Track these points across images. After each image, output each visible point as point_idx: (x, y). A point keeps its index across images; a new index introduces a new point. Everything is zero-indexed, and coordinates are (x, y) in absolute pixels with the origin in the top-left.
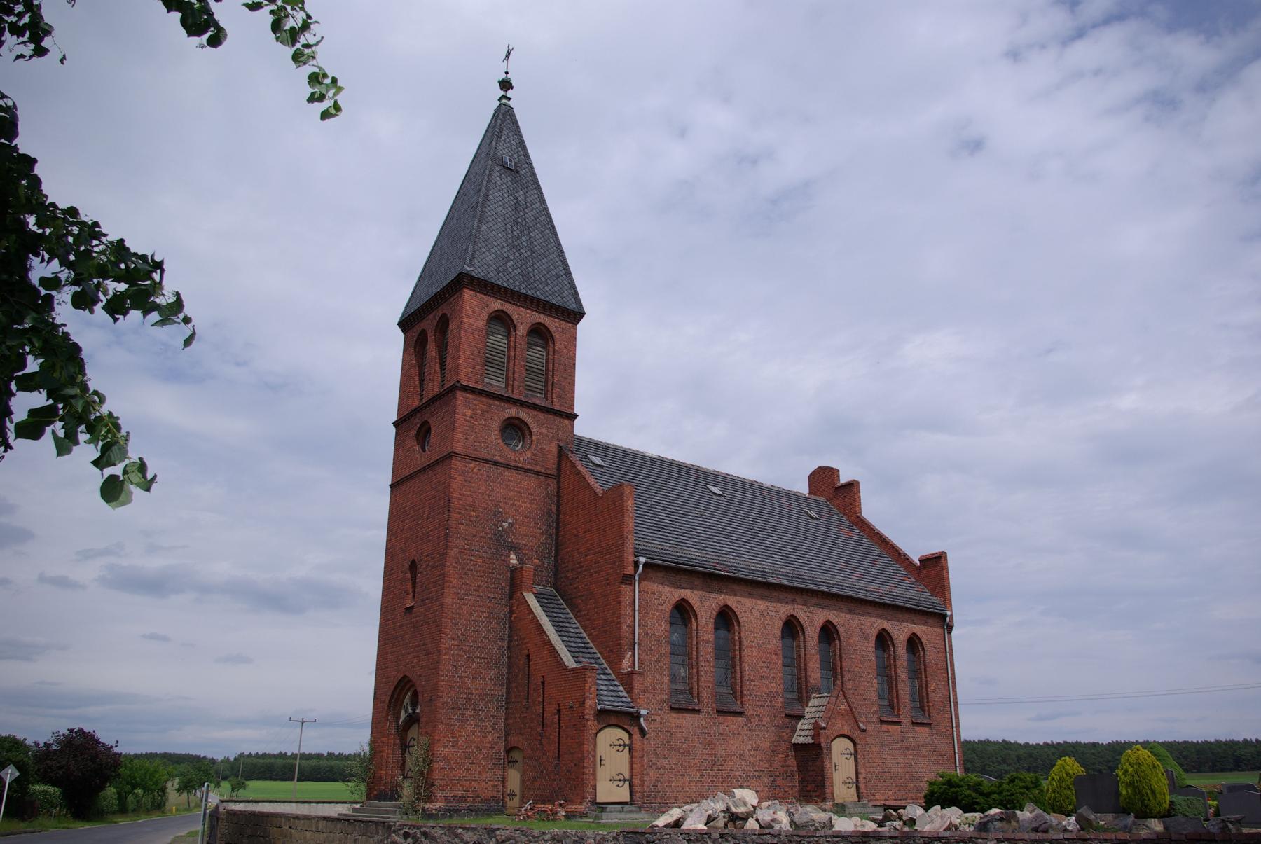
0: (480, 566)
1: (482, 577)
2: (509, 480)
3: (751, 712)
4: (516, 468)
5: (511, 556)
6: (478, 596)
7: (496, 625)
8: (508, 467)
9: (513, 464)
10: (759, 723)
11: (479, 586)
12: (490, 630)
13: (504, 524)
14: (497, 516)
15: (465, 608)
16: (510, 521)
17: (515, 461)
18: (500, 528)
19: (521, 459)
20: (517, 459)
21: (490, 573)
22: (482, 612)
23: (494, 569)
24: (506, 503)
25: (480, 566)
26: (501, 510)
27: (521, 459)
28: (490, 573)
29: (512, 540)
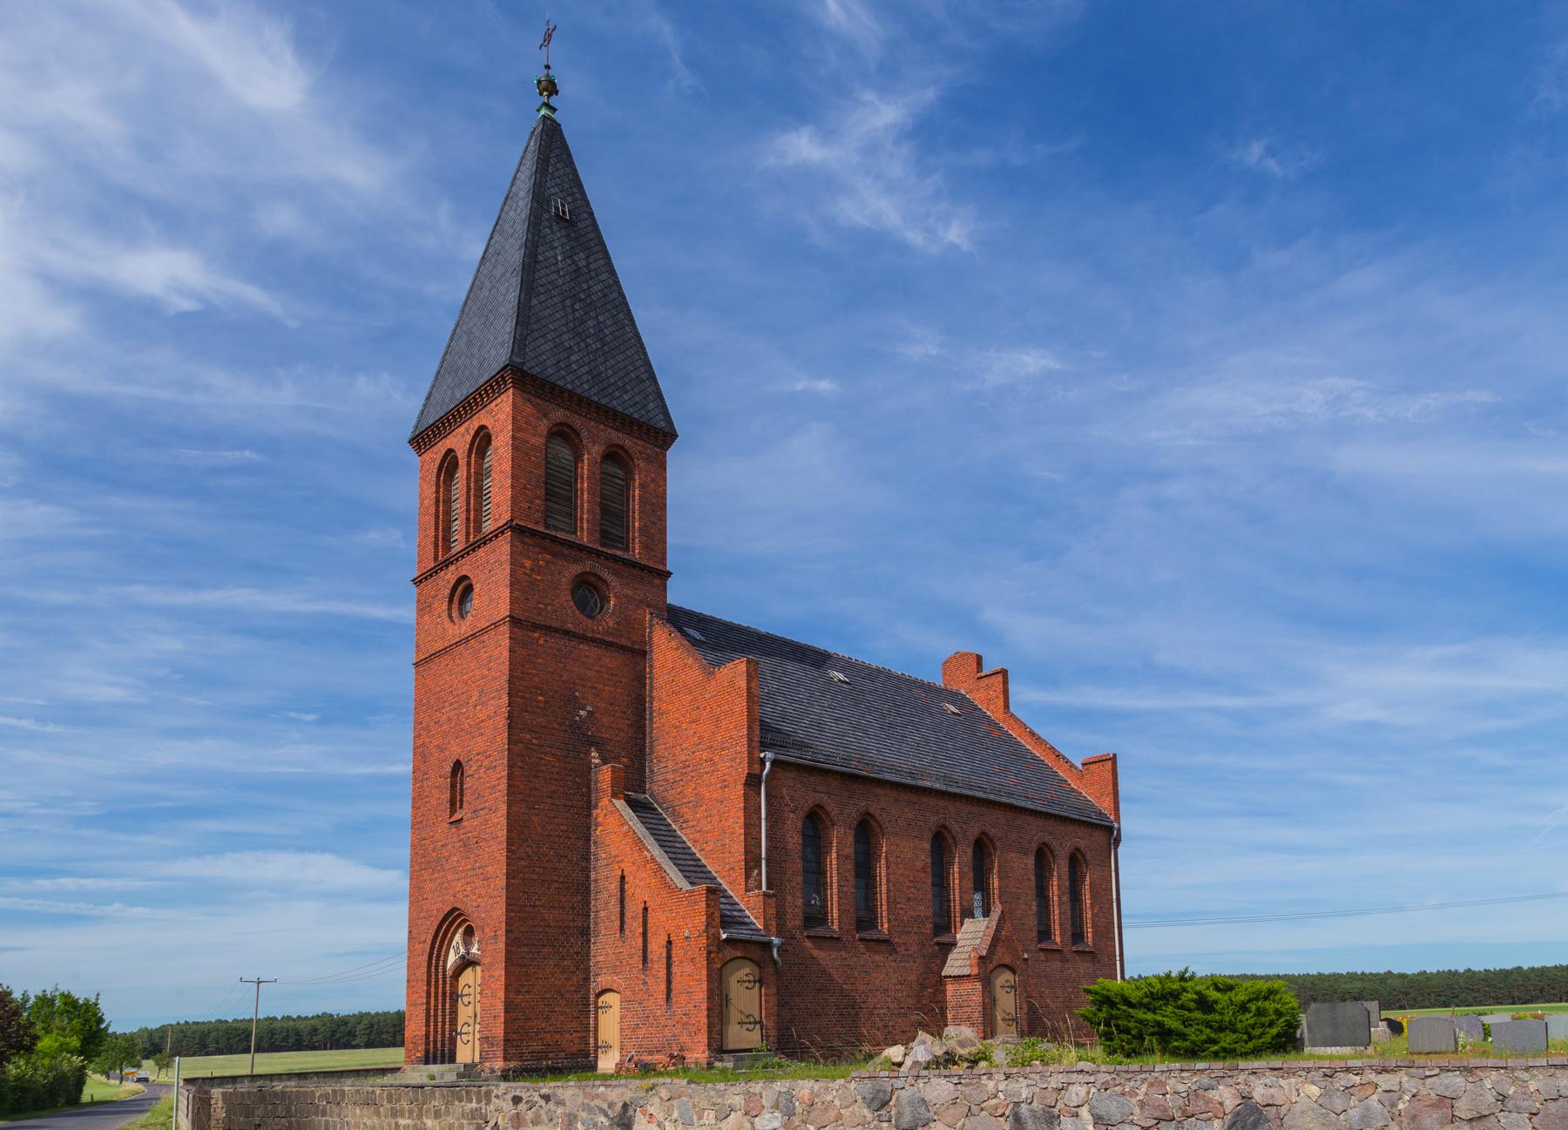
0: (553, 766)
1: (556, 779)
2: (586, 656)
3: (897, 940)
4: (593, 640)
5: (593, 754)
6: (552, 804)
7: (576, 841)
8: (583, 639)
9: (589, 635)
10: (906, 953)
11: (553, 792)
12: (569, 847)
13: (582, 713)
14: (574, 703)
15: (535, 819)
16: (589, 708)
17: (593, 631)
18: (577, 718)
19: (600, 628)
20: (595, 628)
21: (566, 775)
22: (558, 824)
23: (570, 770)
24: (583, 685)
25: (553, 766)
26: (577, 694)
27: (600, 628)
28: (566, 775)
29: (592, 733)
